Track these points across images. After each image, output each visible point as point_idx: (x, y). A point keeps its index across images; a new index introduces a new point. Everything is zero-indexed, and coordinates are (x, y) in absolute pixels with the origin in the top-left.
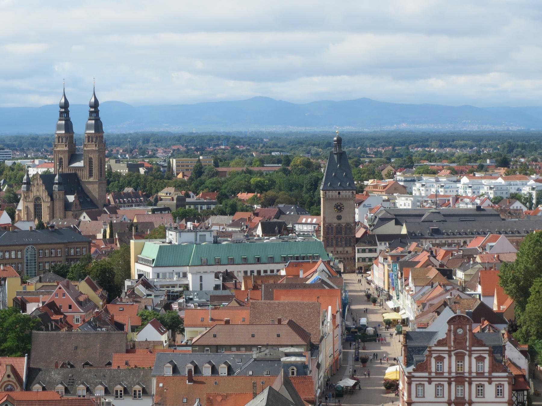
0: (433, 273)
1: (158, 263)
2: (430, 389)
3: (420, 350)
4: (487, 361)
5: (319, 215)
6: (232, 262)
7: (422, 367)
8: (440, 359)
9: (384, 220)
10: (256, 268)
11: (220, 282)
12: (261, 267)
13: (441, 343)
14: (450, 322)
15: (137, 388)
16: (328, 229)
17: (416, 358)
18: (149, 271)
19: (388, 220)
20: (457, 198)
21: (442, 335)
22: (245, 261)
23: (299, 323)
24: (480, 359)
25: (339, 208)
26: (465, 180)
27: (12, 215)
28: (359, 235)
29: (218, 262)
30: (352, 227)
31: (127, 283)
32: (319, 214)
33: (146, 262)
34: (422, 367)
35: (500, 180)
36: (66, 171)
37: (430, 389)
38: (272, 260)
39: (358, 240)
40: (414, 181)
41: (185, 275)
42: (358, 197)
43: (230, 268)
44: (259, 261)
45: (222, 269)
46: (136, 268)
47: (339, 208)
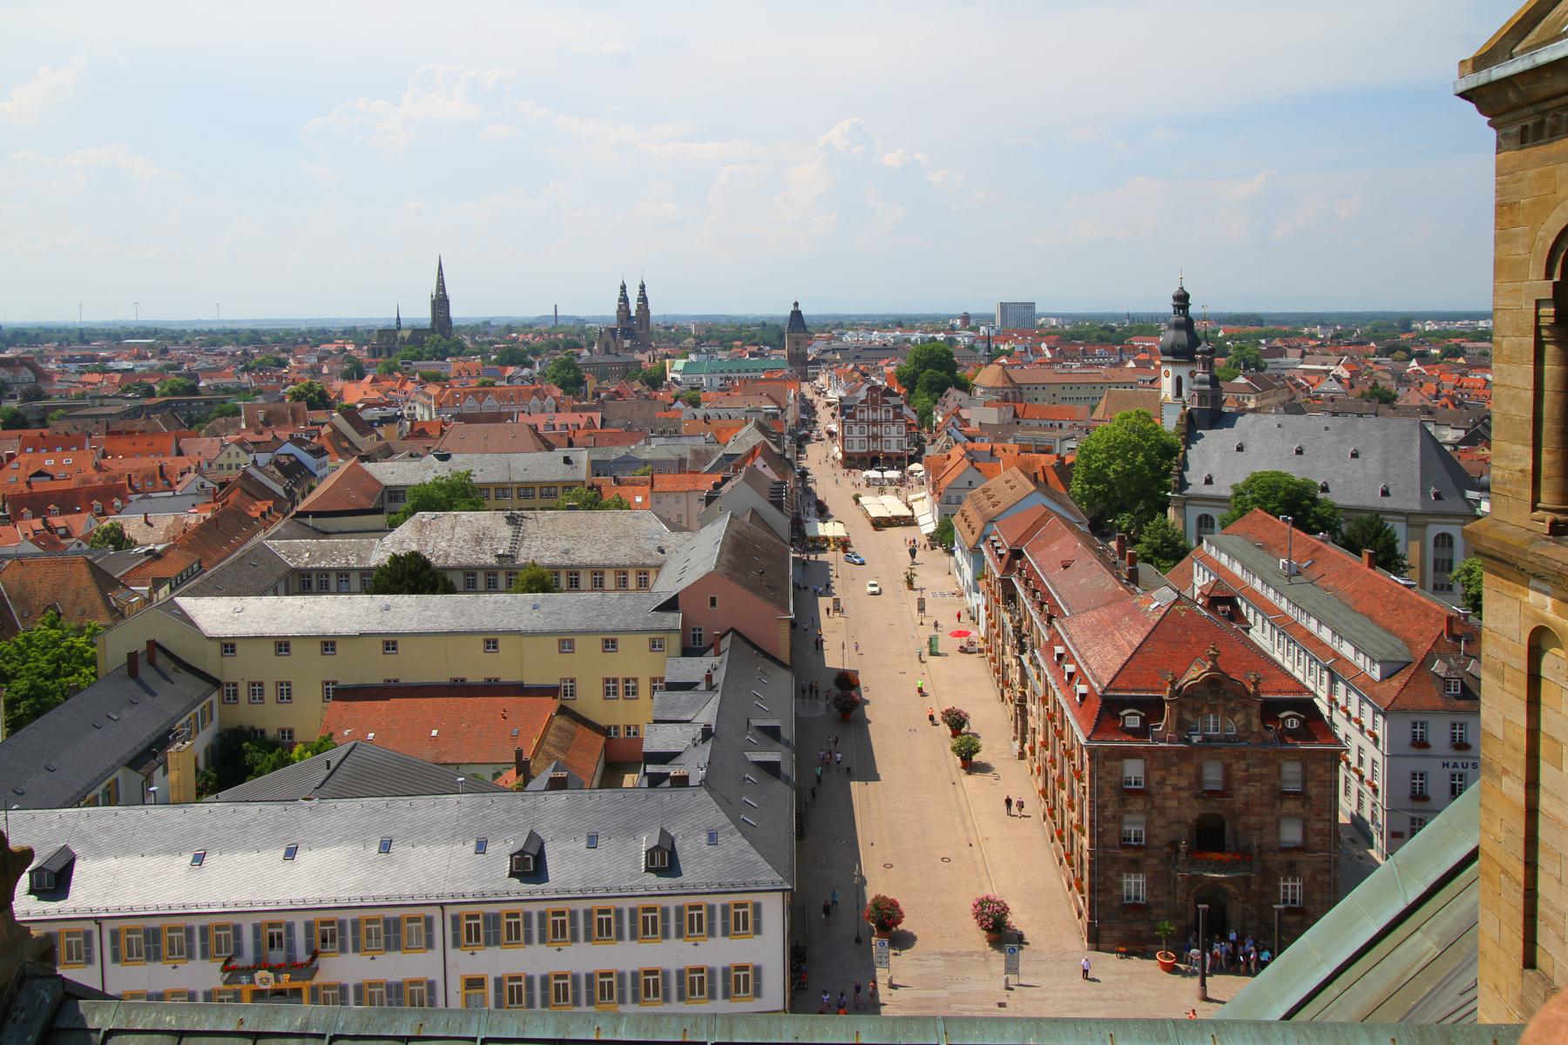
0: (856, 375)
1: (683, 372)
2: (856, 430)
3: (850, 407)
4: (891, 413)
5: (784, 348)
6: (730, 371)
7: (852, 416)
8: (862, 411)
9: (825, 351)
10: (745, 375)
11: (723, 382)
12: (749, 375)
13: (862, 402)
14: (868, 390)
15: (672, 429)
16: (790, 355)
17: (847, 411)
18: (677, 376)
19: (828, 351)
20: (871, 342)
21: (864, 398)
22: (739, 371)
23: (773, 396)
24: (887, 411)
25: (797, 343)
26: (875, 333)
27: (590, 351)
28: (810, 359)
29: (722, 372)
30: (805, 355)
31: (664, 383)
32: (784, 348)
33: (676, 371)
34: (852, 416)
35: (897, 333)
36: (626, 326)
37: (856, 430)
38: (755, 371)
39: (810, 363)
40: (843, 334)
41: (701, 379)
42: (809, 342)
43: (729, 375)
44: (747, 371)
45: (724, 375)
46: (670, 376)
47: (797, 343)
